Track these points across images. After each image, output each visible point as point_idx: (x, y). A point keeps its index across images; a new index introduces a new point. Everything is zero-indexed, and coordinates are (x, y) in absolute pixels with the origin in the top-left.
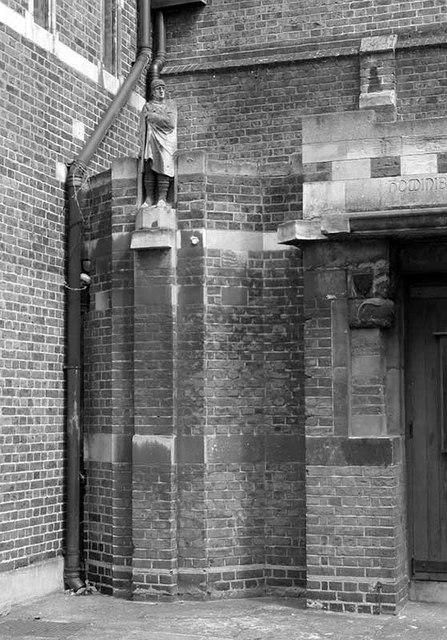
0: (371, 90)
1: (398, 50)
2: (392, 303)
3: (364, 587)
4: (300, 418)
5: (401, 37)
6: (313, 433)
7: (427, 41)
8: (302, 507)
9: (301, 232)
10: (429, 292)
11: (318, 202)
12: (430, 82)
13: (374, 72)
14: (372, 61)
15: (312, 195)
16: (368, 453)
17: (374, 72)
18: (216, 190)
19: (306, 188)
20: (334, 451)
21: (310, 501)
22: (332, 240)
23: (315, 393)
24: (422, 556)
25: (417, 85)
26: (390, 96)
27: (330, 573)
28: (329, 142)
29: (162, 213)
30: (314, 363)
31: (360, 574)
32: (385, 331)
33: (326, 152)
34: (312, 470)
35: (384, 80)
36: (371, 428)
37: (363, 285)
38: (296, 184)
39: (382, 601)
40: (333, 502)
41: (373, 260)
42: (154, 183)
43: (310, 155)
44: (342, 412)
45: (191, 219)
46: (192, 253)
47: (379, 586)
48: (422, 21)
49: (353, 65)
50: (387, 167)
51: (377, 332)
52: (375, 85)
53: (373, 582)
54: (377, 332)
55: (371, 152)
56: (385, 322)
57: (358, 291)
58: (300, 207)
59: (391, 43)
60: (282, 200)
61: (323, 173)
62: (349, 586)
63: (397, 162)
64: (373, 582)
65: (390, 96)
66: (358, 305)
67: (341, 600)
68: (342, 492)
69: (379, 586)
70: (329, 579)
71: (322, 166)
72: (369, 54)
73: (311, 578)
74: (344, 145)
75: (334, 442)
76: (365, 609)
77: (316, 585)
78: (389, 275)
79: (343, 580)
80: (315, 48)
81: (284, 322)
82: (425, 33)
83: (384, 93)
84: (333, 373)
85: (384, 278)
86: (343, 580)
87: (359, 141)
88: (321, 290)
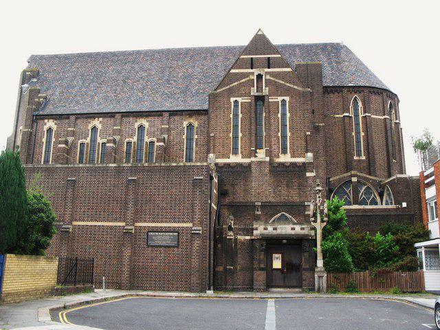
9: (253, 238)
15: (255, 232)
18: (240, 230)
29: (231, 233)
33: (257, 226)
36: (262, 266)
38: (253, 229)
42: (230, 228)
43: (255, 226)
45: (236, 234)
46: (236, 239)
48: (264, 200)
49: (254, 207)
50: (266, 229)
52: (258, 211)
59: (260, 204)
60: (249, 231)
61: (257, 229)
65: (260, 213)
82: (266, 202)
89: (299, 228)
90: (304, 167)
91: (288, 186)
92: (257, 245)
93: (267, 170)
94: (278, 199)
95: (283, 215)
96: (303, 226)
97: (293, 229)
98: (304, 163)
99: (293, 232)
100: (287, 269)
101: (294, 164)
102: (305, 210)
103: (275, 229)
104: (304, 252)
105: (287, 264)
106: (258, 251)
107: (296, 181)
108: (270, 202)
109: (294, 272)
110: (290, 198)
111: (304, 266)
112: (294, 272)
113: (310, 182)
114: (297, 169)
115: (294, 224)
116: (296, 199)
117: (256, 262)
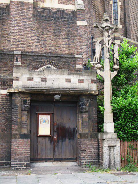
0: (16, 62)
1: (21, 55)
2: (30, 106)
3: (23, 164)
4: (11, 129)
5: (22, 52)
6: (14, 132)
7: (27, 54)
8: (11, 148)
9: (12, 90)
10: (35, 104)
11: (16, 84)
12: (28, 62)
13: (17, 58)
14: (16, 56)
15: (15, 83)
16: (24, 136)
17: (17, 58)
19: (14, 81)
20: (18, 136)
21: (12, 147)
22: (20, 93)
23: (14, 124)
24: (32, 158)
25: (25, 62)
26: (19, 64)
27: (16, 161)
28: (19, 73)
30: (14, 118)
31: (23, 161)
32: (28, 111)
34: (13, 140)
35: (19, 60)
36: (25, 131)
37: (25, 102)
38: (11, 80)
39: (27, 167)
40: (17, 147)
41: (27, 97)
43: (15, 75)
44: (21, 128)
47: (27, 164)
48: (26, 50)
49: (11, 56)
51: (27, 112)
52: (17, 61)
53: (25, 163)
54: (27, 112)
55: (28, 76)
56: (29, 110)
57: (24, 103)
58: (12, 85)
59: (20, 53)
61: (17, 79)
62: (20, 164)
63: (33, 78)
64: (25, 163)
66: (24, 106)
67: (18, 168)
68: (19, 144)
69: (27, 164)
70: (16, 163)
71: (17, 77)
72: (16, 54)
73: (12, 163)
74: (22, 73)
75: (18, 134)
76: (23, 169)
77: (13, 164)
78: (30, 101)
79: (19, 163)
80: (4, 51)
81: (4, 109)
82: (27, 52)
83: (19, 63)
84: (18, 120)
85: (29, 101)
86: (19, 163)
87: (25, 73)
88: (16, 103)
89: (72, 81)
90: (74, 15)
91: (54, 34)
92: (18, 101)
93: (30, 14)
94: (43, 50)
95: (49, 68)
96: (82, 78)
97: (68, 81)
98: (73, 12)
99: (68, 85)
100: (58, 136)
101: (62, 12)
102: (75, 64)
103: (44, 80)
104: (81, 112)
105: (58, 129)
106: (19, 109)
107: (64, 30)
108: (32, 52)
109: (67, 140)
110: (57, 48)
111: (82, 130)
112: (67, 140)
113: (81, 31)
114: (65, 16)
115: (69, 74)
116: (64, 50)
117: (15, 127)
